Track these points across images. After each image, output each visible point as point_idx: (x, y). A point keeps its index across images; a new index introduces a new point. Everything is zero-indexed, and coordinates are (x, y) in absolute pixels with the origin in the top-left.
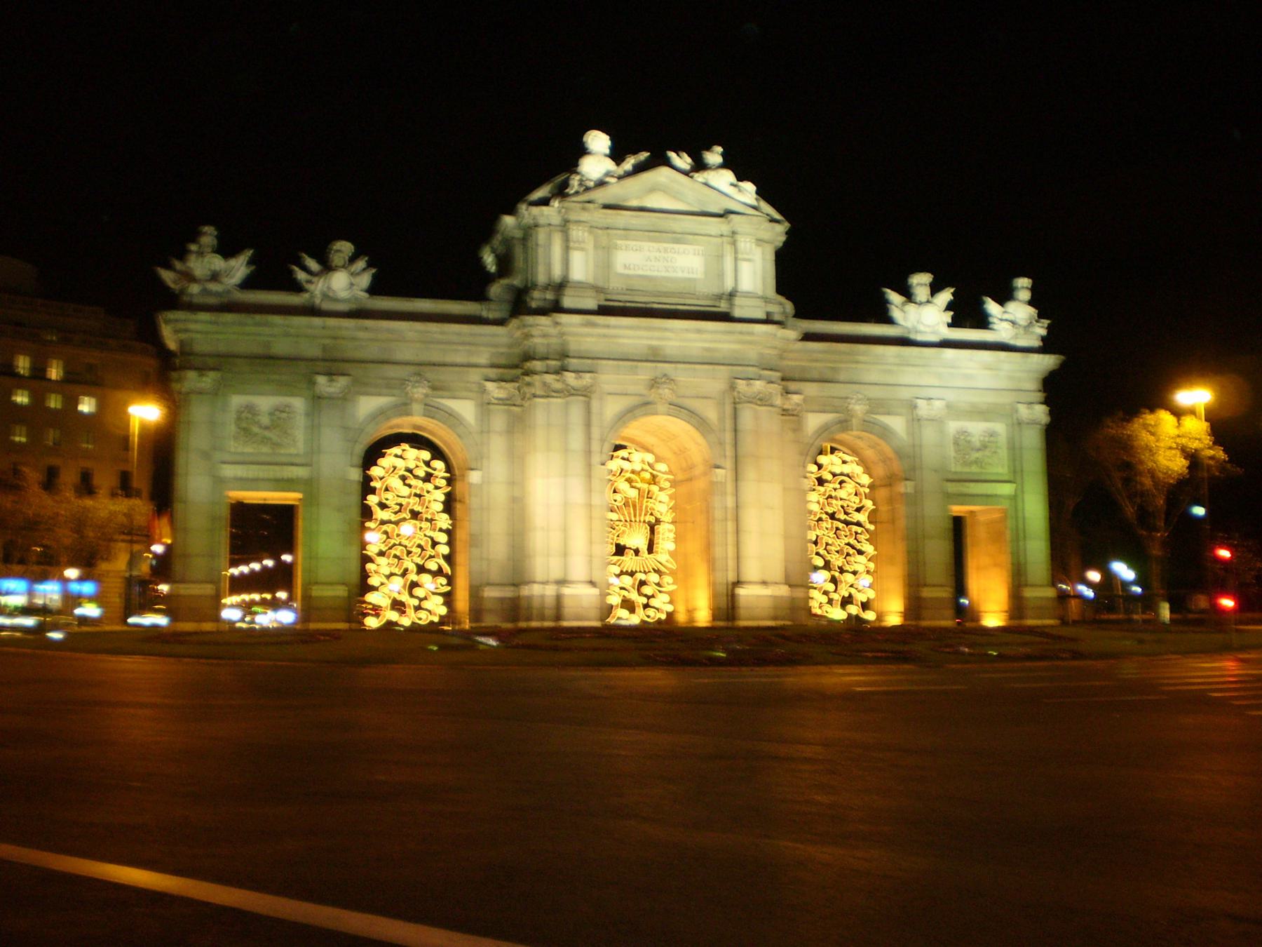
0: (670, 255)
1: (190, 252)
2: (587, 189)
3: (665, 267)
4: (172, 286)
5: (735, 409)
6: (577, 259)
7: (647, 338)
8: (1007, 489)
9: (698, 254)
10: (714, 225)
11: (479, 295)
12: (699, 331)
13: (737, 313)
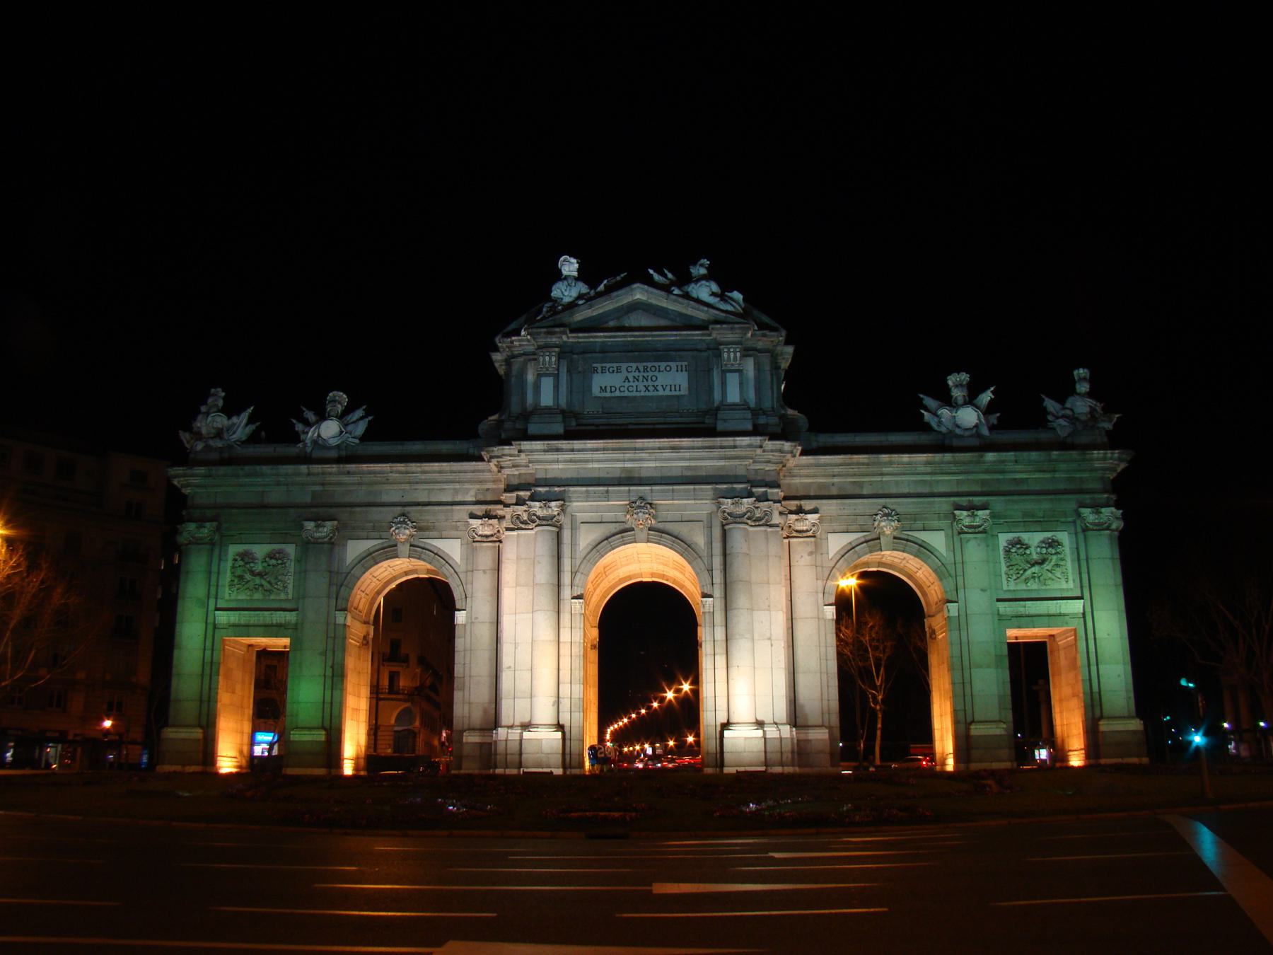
0: (650, 374)
1: (200, 412)
3: (645, 386)
6: (547, 385)
7: (618, 460)
8: (1077, 606)
12: (673, 448)
13: (720, 426)
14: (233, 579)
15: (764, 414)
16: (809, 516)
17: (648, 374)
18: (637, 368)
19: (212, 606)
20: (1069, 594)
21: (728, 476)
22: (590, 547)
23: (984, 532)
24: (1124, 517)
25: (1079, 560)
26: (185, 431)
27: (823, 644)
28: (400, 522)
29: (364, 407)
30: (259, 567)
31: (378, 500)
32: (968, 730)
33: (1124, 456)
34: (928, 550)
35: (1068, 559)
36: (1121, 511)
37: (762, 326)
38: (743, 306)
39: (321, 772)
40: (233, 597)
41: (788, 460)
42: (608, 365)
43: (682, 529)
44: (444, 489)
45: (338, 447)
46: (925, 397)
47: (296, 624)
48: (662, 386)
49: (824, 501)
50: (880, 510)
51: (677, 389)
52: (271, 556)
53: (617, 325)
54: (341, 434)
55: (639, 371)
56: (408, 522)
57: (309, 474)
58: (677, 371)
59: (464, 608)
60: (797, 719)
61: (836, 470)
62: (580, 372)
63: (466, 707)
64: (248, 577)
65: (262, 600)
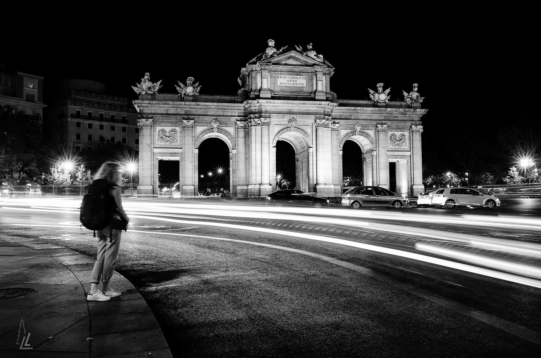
0: (295, 79)
4: (136, 92)
5: (316, 129)
6: (265, 81)
8: (408, 153)
10: (309, 69)
11: (235, 94)
13: (317, 98)
17: (294, 79)
19: (152, 147)
24: (423, 128)
28: (215, 121)
30: (168, 134)
31: (207, 114)
35: (407, 140)
37: (329, 67)
40: (159, 143)
42: (282, 76)
45: (193, 96)
49: (341, 120)
54: (193, 92)
57: (185, 105)
63: (237, 178)
64: (164, 137)
65: (169, 145)
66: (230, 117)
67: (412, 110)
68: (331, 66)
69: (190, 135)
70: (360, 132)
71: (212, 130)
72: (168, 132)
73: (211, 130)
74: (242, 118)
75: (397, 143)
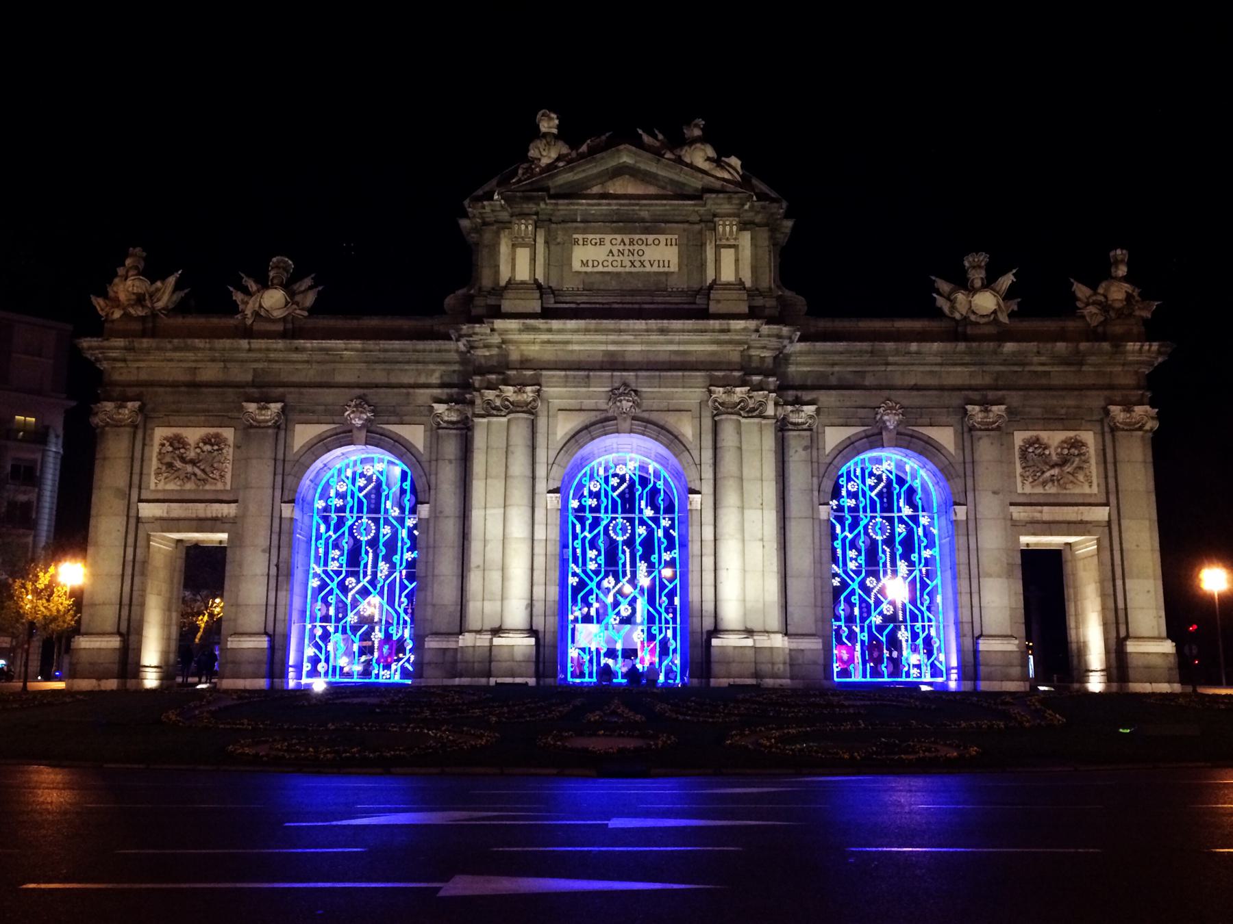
0: (637, 247)
1: (116, 275)
2: (533, 175)
3: (631, 261)
4: (100, 313)
7: (601, 343)
8: (1101, 514)
9: (671, 245)
12: (662, 331)
13: (713, 308)
14: (160, 466)
15: (761, 295)
16: (805, 408)
18: (623, 241)
19: (134, 497)
20: (1092, 500)
21: (720, 363)
22: (568, 437)
23: (999, 428)
24: (1159, 417)
25: (1105, 462)
26: (99, 296)
27: (817, 547)
29: (313, 275)
30: (191, 454)
32: (975, 644)
33: (1163, 349)
34: (934, 447)
35: (1093, 461)
36: (1157, 410)
37: (762, 197)
38: (741, 173)
39: (262, 683)
40: (160, 487)
41: (785, 346)
42: (590, 237)
43: (670, 420)
44: (406, 370)
45: (284, 319)
46: (937, 280)
47: (236, 517)
48: (650, 261)
49: (823, 392)
50: (883, 403)
51: (666, 265)
52: (207, 440)
53: (601, 192)
55: (625, 244)
56: (366, 406)
57: (250, 350)
58: (667, 245)
59: (427, 500)
60: (788, 627)
61: (836, 358)
62: (559, 244)
64: (178, 464)
66: (411, 390)
67: (1106, 346)
68: (773, 195)
69: (269, 454)
70: (898, 433)
71: (348, 437)
72: (193, 445)
73: (343, 438)
74: (455, 390)
75: (1052, 472)
